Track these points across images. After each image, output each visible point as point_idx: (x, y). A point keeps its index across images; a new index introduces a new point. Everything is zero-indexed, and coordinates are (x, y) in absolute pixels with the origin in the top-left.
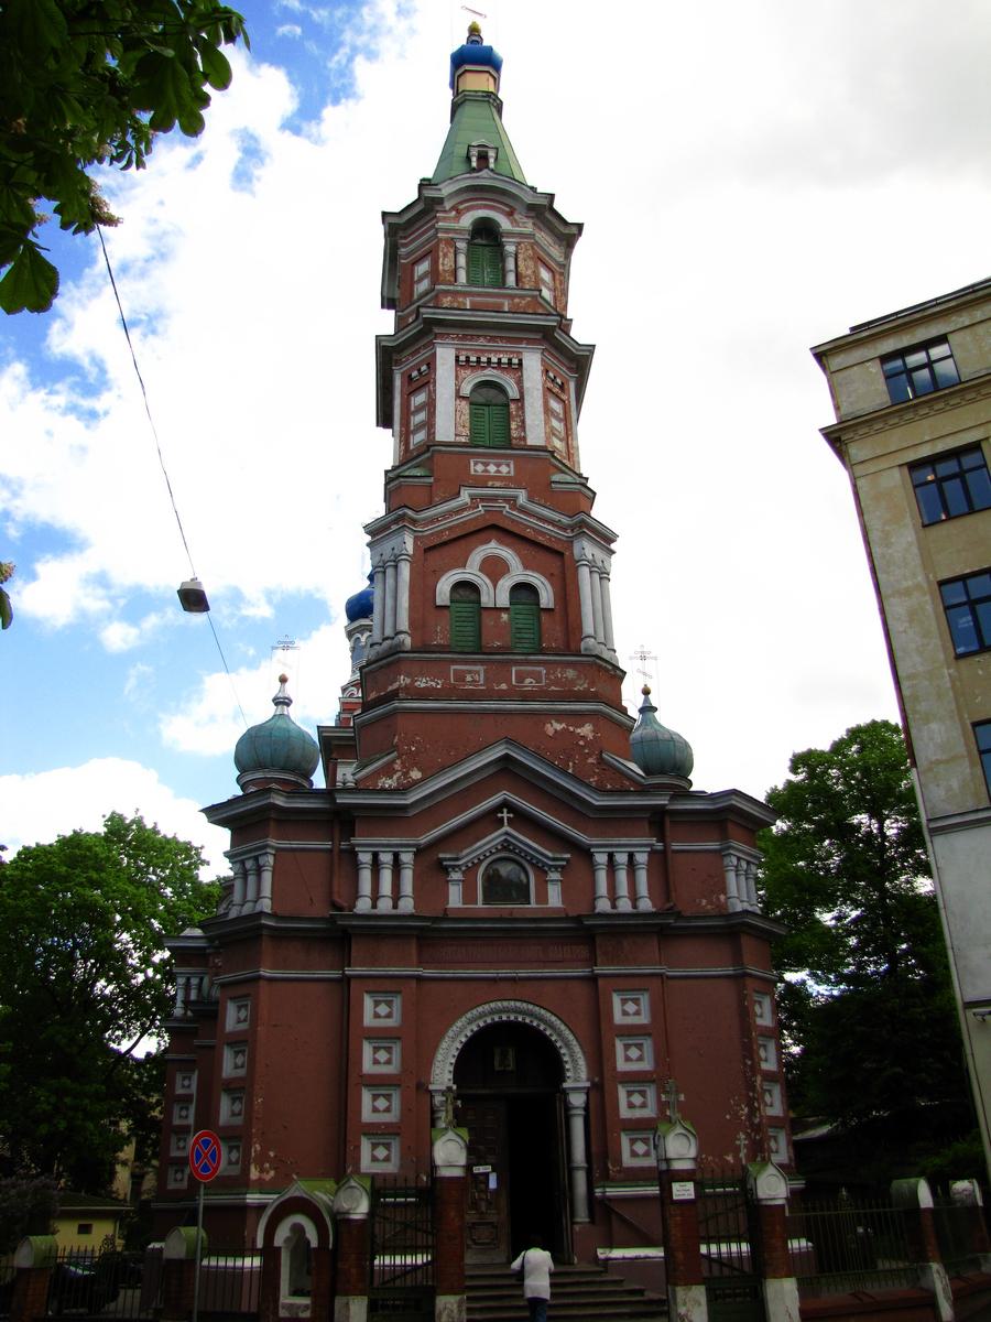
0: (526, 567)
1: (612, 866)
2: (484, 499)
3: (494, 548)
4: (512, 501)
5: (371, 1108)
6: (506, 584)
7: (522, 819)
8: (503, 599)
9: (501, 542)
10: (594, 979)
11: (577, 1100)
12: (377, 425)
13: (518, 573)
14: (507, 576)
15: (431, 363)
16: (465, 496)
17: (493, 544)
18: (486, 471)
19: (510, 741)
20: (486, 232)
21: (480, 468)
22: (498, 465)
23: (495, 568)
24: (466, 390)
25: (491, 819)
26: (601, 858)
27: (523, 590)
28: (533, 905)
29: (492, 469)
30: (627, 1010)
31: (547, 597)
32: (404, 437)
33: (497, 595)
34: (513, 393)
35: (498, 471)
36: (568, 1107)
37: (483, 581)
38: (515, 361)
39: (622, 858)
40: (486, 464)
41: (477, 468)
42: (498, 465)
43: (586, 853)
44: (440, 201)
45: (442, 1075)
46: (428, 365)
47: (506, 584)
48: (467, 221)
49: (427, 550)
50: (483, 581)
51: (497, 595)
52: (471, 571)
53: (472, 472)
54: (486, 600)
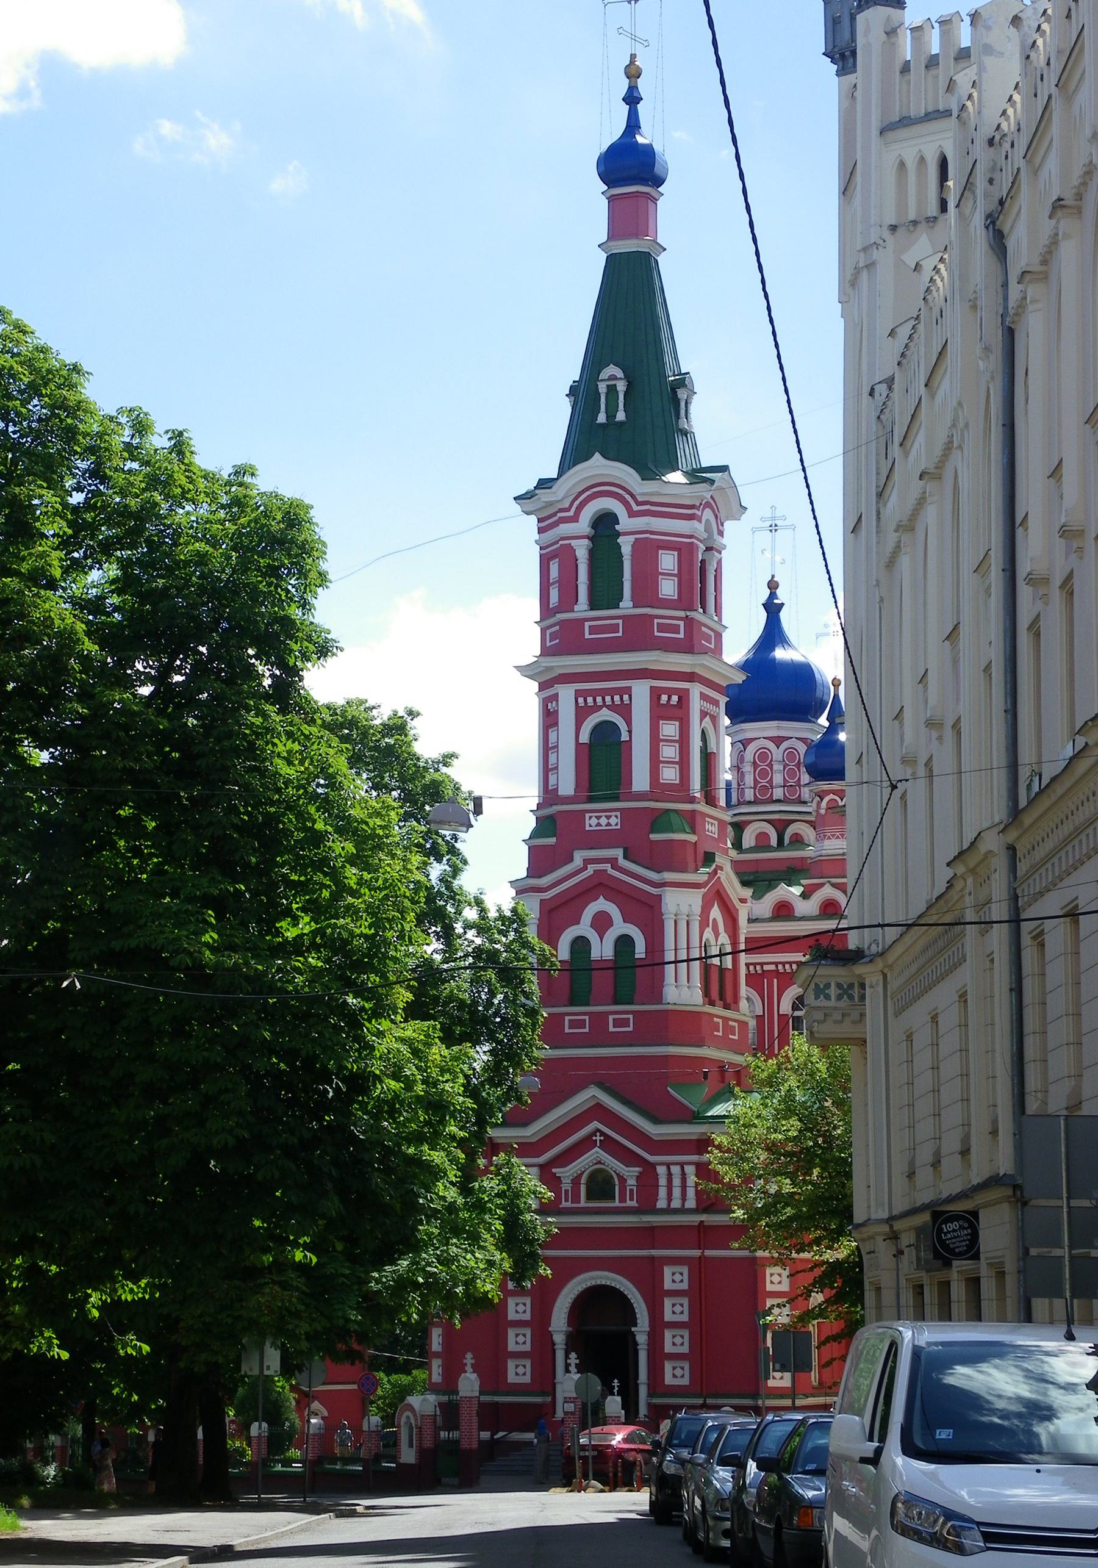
1: (670, 1176)
3: (601, 904)
4: (613, 862)
5: (518, 1340)
6: (611, 935)
7: (609, 1145)
10: (652, 1258)
11: (642, 1339)
13: (620, 927)
17: (601, 899)
18: (599, 824)
19: (601, 1085)
20: (605, 523)
21: (594, 821)
22: (608, 817)
23: (602, 923)
24: (584, 738)
25: (586, 1144)
26: (661, 1170)
27: (624, 943)
28: (617, 1203)
29: (603, 821)
30: (675, 1278)
31: (640, 951)
33: (603, 949)
34: (624, 737)
35: (609, 824)
36: (636, 1344)
37: (592, 936)
39: (676, 1170)
40: (598, 818)
41: (591, 823)
42: (608, 817)
43: (653, 1166)
45: (559, 1322)
47: (611, 935)
48: (583, 525)
49: (550, 911)
50: (592, 936)
51: (603, 949)
52: (584, 928)
53: (588, 828)
54: (595, 954)
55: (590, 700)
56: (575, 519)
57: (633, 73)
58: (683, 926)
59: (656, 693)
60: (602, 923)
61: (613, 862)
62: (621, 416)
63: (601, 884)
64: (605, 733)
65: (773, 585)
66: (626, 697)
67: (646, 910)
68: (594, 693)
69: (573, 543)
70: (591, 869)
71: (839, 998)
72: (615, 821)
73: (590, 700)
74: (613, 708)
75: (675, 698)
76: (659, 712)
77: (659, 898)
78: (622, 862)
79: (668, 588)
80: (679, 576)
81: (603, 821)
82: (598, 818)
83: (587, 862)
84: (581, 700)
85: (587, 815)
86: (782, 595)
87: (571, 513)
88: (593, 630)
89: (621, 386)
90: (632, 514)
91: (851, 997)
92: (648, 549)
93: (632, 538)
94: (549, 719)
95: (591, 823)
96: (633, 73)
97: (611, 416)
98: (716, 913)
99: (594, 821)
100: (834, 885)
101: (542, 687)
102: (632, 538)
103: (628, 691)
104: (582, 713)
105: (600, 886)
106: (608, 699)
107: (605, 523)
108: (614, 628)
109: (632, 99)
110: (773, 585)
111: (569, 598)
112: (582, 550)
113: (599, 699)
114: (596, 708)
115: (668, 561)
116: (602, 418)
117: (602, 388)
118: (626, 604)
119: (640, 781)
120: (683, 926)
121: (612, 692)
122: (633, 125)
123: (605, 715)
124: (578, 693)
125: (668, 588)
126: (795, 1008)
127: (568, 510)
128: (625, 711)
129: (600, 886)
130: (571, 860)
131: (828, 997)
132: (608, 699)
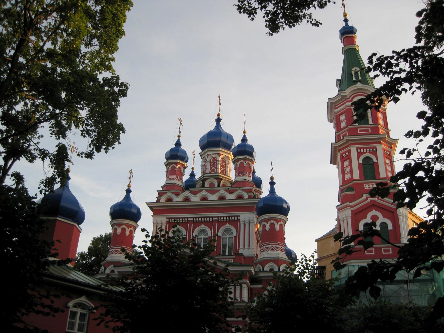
0: (384, 217)
3: (374, 212)
9: (375, 210)
12: (331, 163)
14: (378, 220)
15: (349, 151)
18: (369, 187)
21: (367, 186)
24: (361, 161)
31: (390, 227)
32: (343, 173)
34: (375, 161)
38: (375, 149)
44: (346, 96)
46: (348, 153)
55: (362, 150)
57: (345, 15)
60: (375, 218)
63: (373, 205)
64: (367, 159)
66: (375, 149)
68: (363, 148)
73: (362, 150)
74: (370, 152)
82: (369, 185)
84: (359, 150)
85: (365, 185)
87: (350, 100)
88: (360, 131)
96: (345, 15)
103: (376, 148)
104: (359, 155)
106: (368, 150)
108: (368, 130)
109: (346, 20)
113: (365, 150)
114: (364, 153)
116: (354, 79)
117: (353, 73)
122: (347, 24)
123: (368, 155)
124: (357, 149)
127: (349, 99)
130: (362, 196)
132: (368, 150)
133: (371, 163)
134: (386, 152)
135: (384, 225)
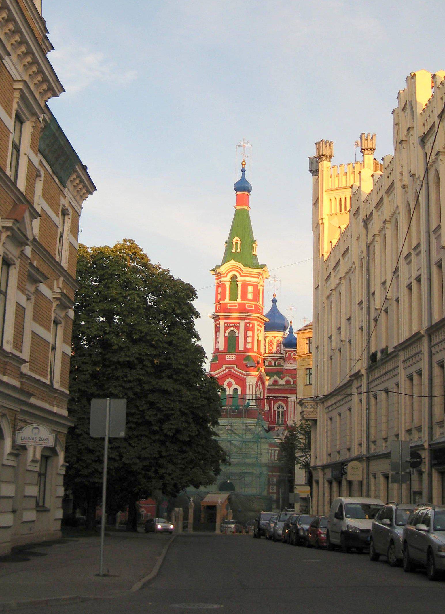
2: (228, 368)
3: (230, 380)
4: (234, 369)
6: (232, 388)
8: (231, 393)
13: (235, 386)
16: (224, 367)
20: (234, 277)
21: (228, 357)
24: (227, 335)
27: (236, 390)
29: (231, 357)
31: (240, 393)
34: (237, 335)
41: (227, 358)
47: (232, 388)
48: (228, 278)
56: (226, 277)
58: (251, 386)
59: (246, 324)
60: (230, 385)
61: (234, 369)
62: (239, 250)
65: (274, 295)
67: (241, 381)
69: (225, 283)
70: (227, 370)
71: (311, 408)
72: (234, 358)
75: (251, 325)
76: (247, 329)
77: (245, 379)
78: (236, 368)
79: (250, 296)
80: (253, 293)
81: (231, 357)
83: (226, 368)
86: (277, 298)
89: (239, 243)
90: (241, 276)
91: (314, 408)
92: (245, 286)
93: (241, 282)
94: (217, 329)
95: (227, 358)
97: (236, 250)
98: (260, 383)
99: (228, 357)
100: (289, 376)
101: (215, 321)
102: (241, 282)
103: (239, 323)
104: (226, 328)
105: (230, 375)
107: (234, 277)
108: (235, 306)
109: (243, 170)
110: (274, 295)
111: (223, 297)
112: (228, 285)
115: (250, 289)
116: (234, 251)
117: (234, 243)
118: (239, 300)
119: (241, 348)
120: (251, 386)
121: (234, 323)
122: (243, 177)
123: (232, 329)
124: (225, 323)
125: (250, 296)
126: (278, 409)
128: (238, 328)
129: (230, 375)
131: (308, 408)
133: (235, 335)
134: (248, 325)
135: (236, 390)
